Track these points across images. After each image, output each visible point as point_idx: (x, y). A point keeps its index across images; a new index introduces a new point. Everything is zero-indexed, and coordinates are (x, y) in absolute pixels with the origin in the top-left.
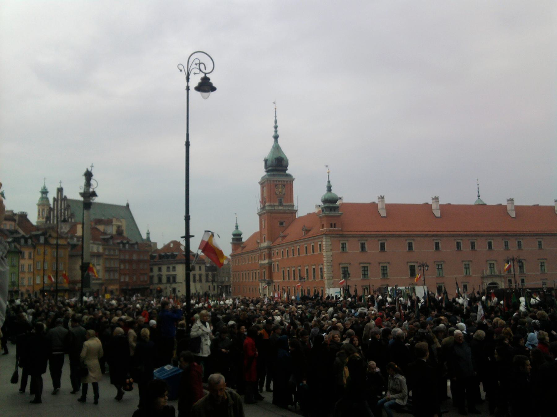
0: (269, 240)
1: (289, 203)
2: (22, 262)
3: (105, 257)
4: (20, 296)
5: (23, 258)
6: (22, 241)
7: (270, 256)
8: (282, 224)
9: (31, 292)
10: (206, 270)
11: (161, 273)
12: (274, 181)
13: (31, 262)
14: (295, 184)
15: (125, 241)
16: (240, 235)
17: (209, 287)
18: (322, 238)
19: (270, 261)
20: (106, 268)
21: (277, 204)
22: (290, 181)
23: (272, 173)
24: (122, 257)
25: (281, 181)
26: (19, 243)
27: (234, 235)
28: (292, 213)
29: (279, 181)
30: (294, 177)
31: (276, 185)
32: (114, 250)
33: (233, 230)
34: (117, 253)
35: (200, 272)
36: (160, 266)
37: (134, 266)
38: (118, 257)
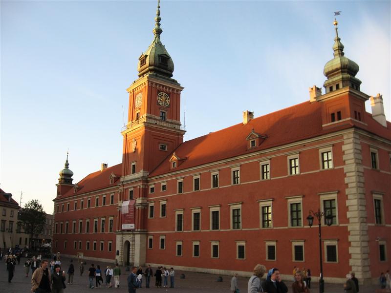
0: (145, 169)
1: (174, 121)
7: (145, 193)
8: (163, 148)
10: (19, 217)
12: (156, 84)
14: (183, 95)
16: (72, 175)
17: (21, 238)
18: (342, 137)
19: (145, 201)
21: (159, 118)
22: (177, 91)
23: (155, 74)
25: (166, 87)
27: (63, 175)
28: (178, 135)
29: (163, 86)
30: (181, 86)
31: (159, 91)
33: (63, 167)
35: (12, 219)
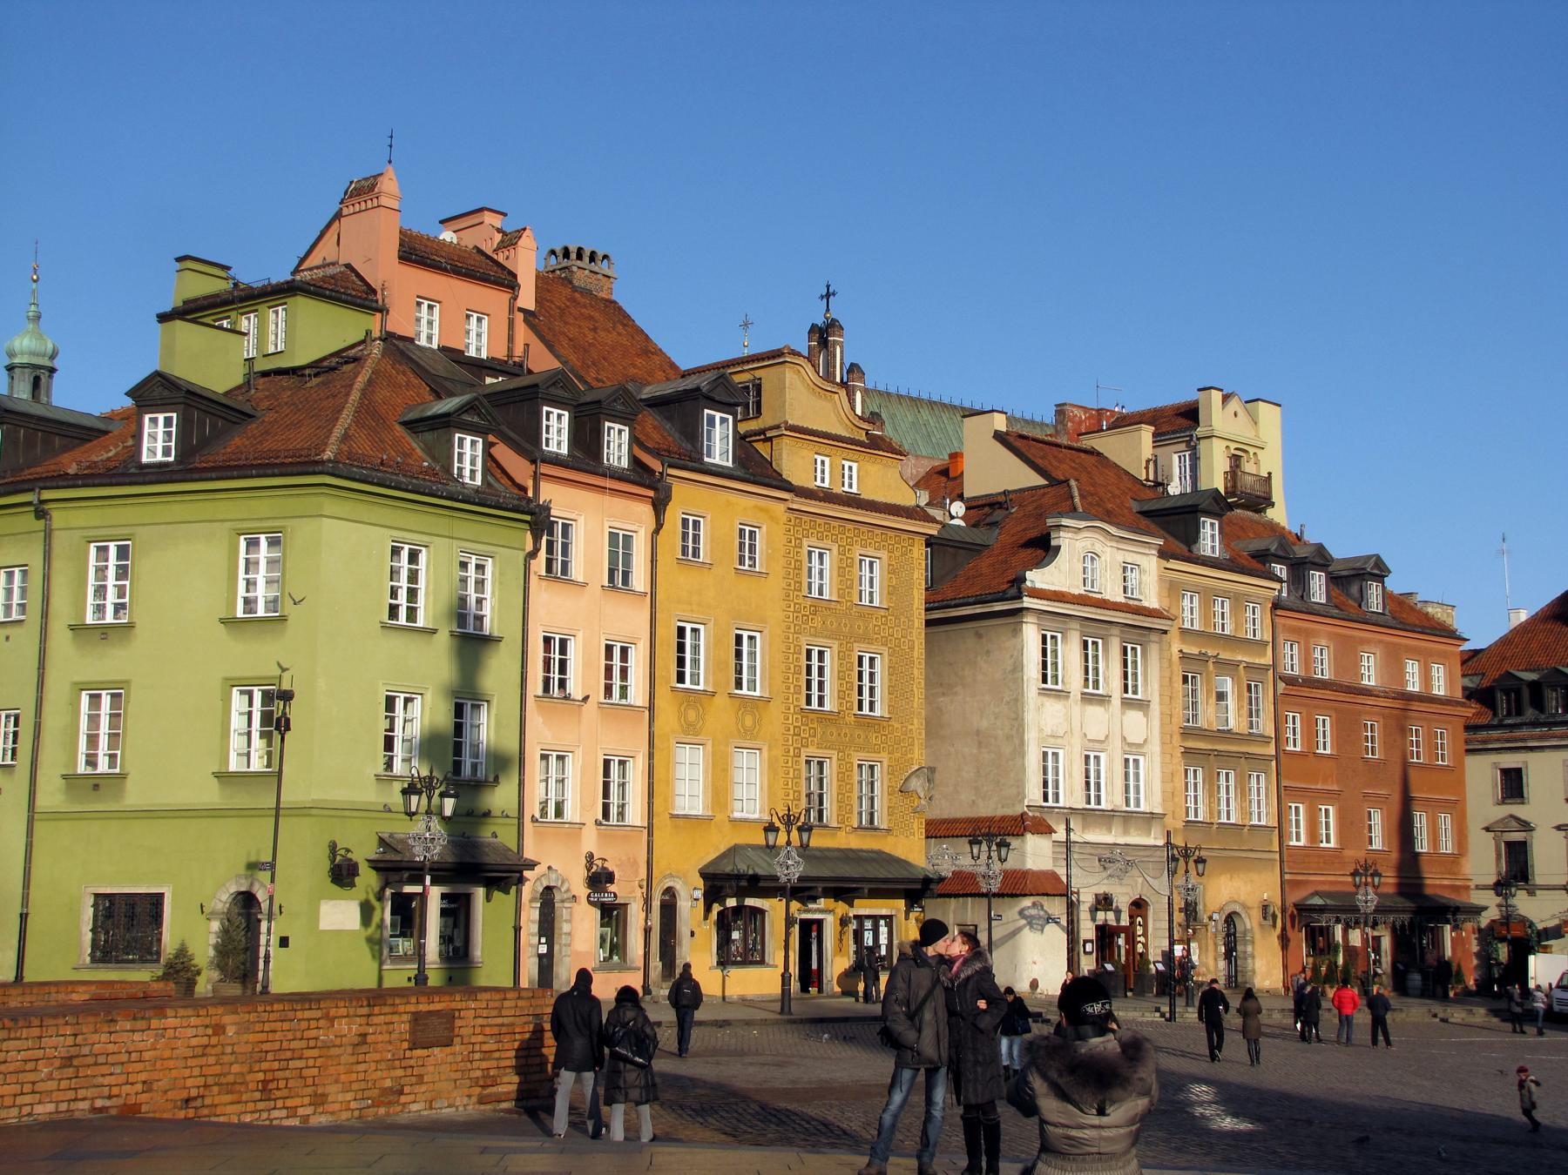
2: (552, 609)
3: (1176, 646)
4: (531, 916)
5: (558, 571)
6: (557, 430)
9: (626, 889)
11: (1520, 811)
13: (628, 621)
15: (1300, 552)
20: (1186, 733)
24: (1292, 663)
26: (528, 442)
32: (1238, 601)
34: (1258, 623)
36: (1511, 760)
37: (1374, 739)
38: (1267, 660)
